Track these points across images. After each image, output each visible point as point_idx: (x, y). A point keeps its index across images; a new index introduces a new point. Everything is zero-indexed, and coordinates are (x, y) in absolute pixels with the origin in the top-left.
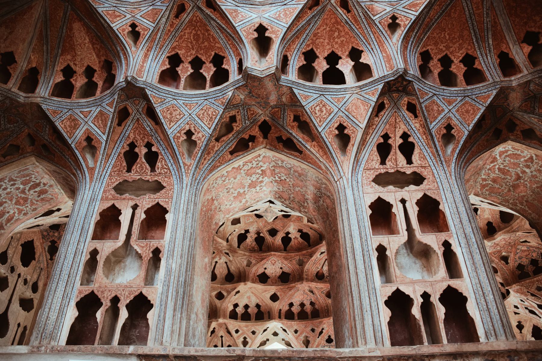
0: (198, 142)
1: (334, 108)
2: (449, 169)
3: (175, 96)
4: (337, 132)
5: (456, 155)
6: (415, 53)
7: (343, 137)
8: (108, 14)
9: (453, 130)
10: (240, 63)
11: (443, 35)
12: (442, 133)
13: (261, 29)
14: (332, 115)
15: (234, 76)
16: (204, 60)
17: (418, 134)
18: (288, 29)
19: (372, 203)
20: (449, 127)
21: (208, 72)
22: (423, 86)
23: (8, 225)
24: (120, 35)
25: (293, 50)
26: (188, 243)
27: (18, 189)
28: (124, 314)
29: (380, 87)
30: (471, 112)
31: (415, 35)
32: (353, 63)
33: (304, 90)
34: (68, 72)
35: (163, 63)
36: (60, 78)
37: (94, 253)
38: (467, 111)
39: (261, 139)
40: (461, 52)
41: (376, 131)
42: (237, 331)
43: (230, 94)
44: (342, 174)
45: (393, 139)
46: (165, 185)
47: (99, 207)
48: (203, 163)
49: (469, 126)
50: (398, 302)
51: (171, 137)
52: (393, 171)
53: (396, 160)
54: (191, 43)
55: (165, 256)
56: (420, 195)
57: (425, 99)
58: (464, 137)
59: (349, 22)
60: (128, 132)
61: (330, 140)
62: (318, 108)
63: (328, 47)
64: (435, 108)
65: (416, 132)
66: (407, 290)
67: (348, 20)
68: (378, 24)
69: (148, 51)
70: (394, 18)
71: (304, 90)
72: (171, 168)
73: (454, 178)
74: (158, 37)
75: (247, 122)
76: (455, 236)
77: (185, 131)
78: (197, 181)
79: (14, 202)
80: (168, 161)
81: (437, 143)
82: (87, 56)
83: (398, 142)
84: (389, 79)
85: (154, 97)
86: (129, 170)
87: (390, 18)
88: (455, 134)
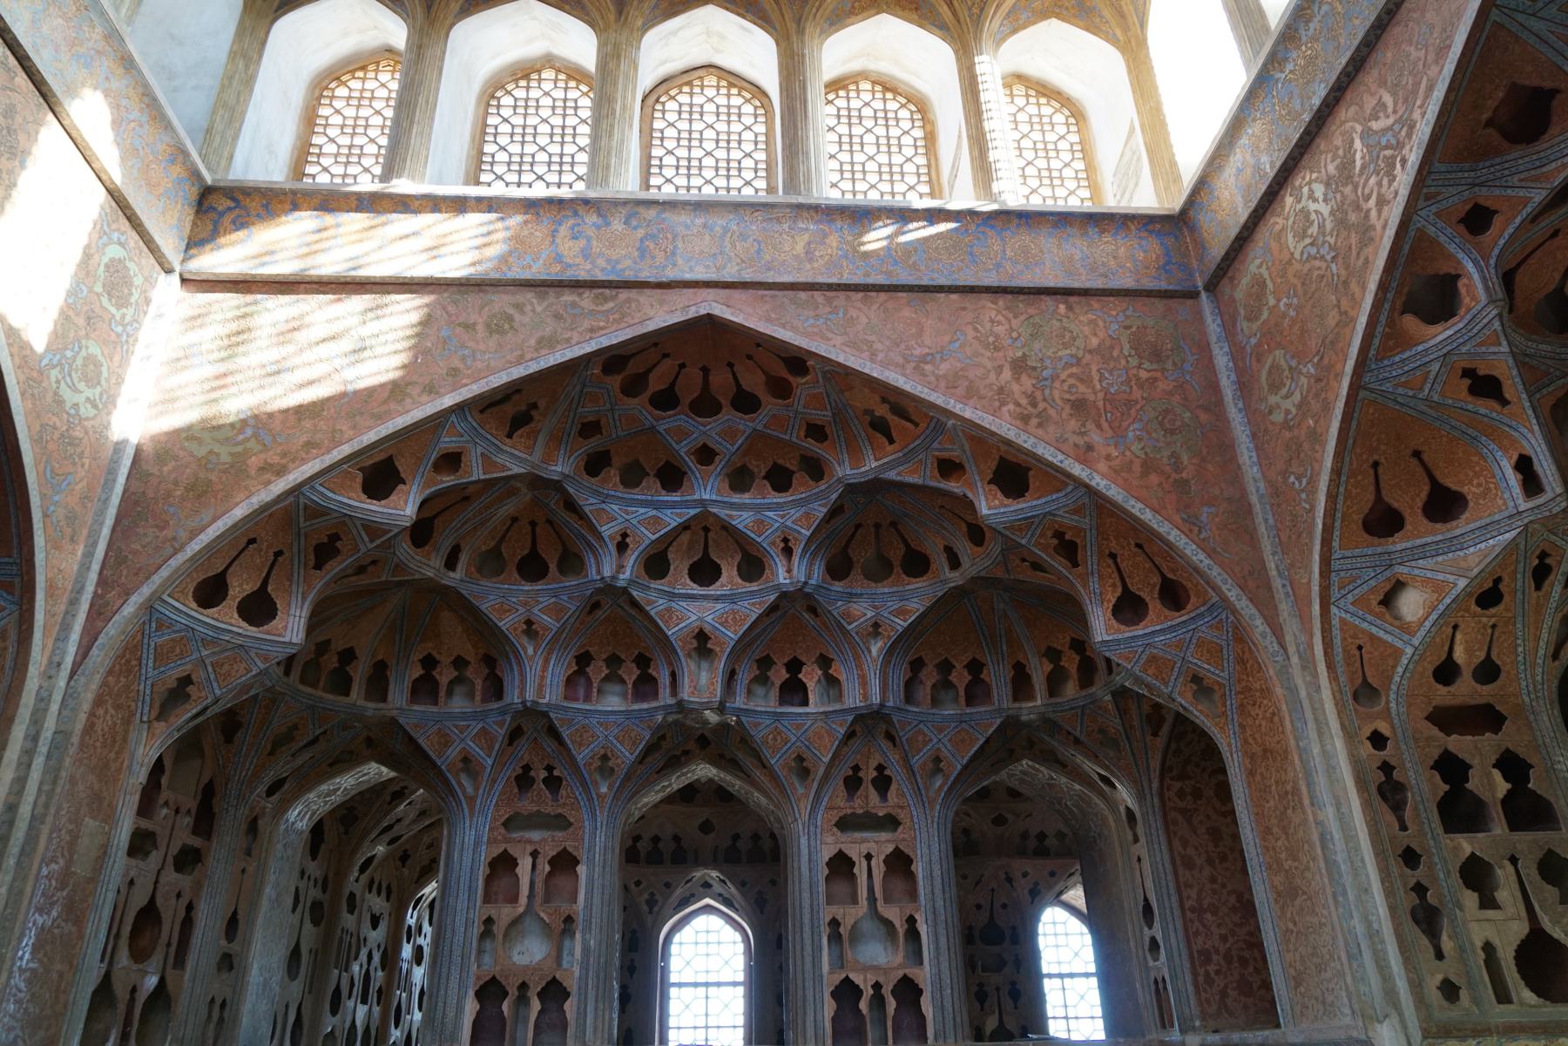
3: (587, 714)
7: (802, 769)
10: (673, 675)
15: (665, 697)
20: (938, 760)
28: (536, 1006)
29: (850, 718)
34: (429, 663)
36: (418, 672)
37: (489, 921)
42: (638, 883)
43: (660, 718)
47: (485, 855)
50: (847, 992)
56: (890, 848)
66: (857, 978)
70: (876, 625)
82: (455, 641)
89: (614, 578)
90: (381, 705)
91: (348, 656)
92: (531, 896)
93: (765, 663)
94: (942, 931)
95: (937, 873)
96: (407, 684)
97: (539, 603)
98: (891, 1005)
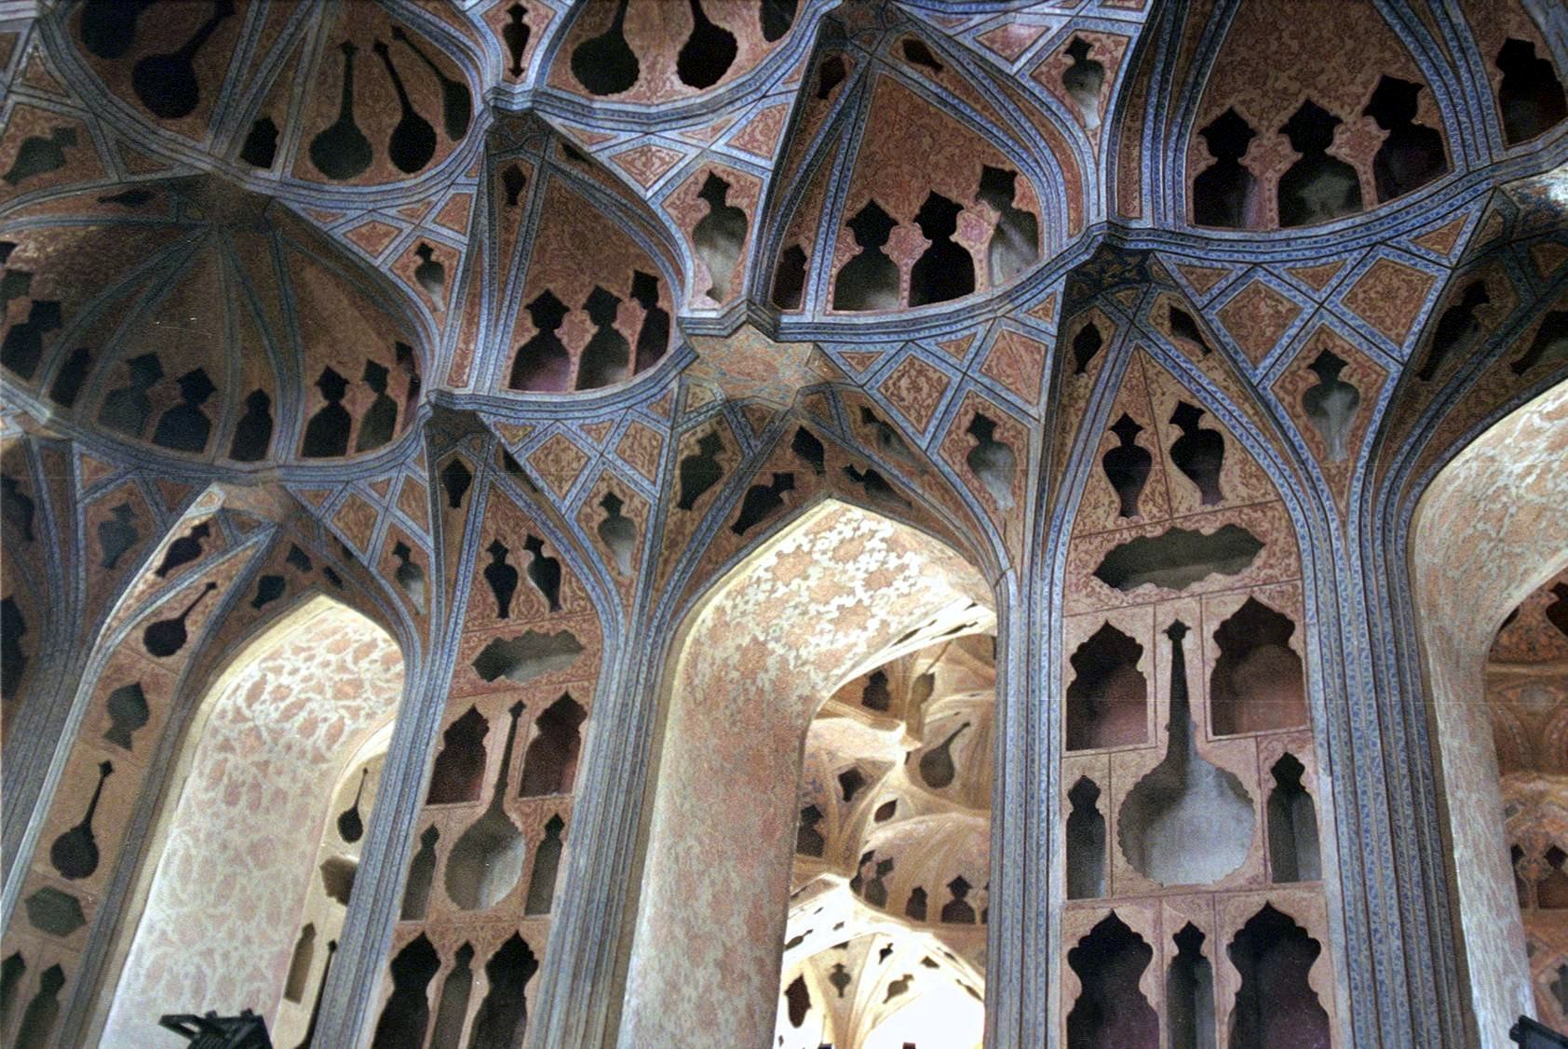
0: (637, 521)
1: (951, 372)
2: (1342, 506)
4: (972, 441)
5: (1365, 453)
6: (1180, 136)
8: (361, 237)
9: (1345, 370)
11: (1274, 46)
12: (1302, 386)
13: (715, 188)
14: (949, 394)
16: (615, 294)
17: (1226, 403)
18: (776, 172)
19: (1082, 647)
20: (1327, 365)
21: (632, 326)
22: (1201, 254)
23: (336, 747)
24: (399, 282)
25: (814, 226)
26: (622, 798)
27: (326, 664)
29: (1060, 287)
30: (1403, 293)
31: (1164, 81)
32: (994, 216)
33: (855, 339)
34: (333, 385)
35: (520, 328)
36: (318, 403)
38: (1389, 295)
39: (813, 478)
40: (1360, 78)
41: (1090, 415)
44: (1005, 563)
45: (1150, 429)
46: (583, 640)
48: (663, 575)
49: (1401, 345)
51: (570, 518)
52: (1159, 531)
53: (1168, 496)
54: (573, 257)
55: (571, 836)
57: (1215, 292)
58: (1390, 386)
59: (950, 100)
60: (480, 519)
61: (957, 468)
62: (904, 383)
63: (915, 184)
64: (1265, 309)
65: (1219, 395)
66: (1136, 919)
67: (944, 95)
68: (1031, 84)
69: (473, 305)
70: (1078, 48)
71: (855, 339)
72: (593, 596)
73: (1353, 532)
74: (486, 265)
75: (753, 443)
76: (1321, 737)
77: (600, 499)
78: (655, 623)
79: (329, 693)
80: (583, 578)
81: (1287, 422)
83: (1167, 436)
84: (1077, 262)
85: (505, 427)
86: (504, 613)
87: (1067, 52)
88: (1353, 381)
89: (497, 91)
90: (258, 464)
91: (198, 386)
92: (501, 786)
93: (872, 226)
94: (1371, 783)
95: (1356, 642)
96: (300, 427)
97: (430, 206)
98: (1227, 982)
